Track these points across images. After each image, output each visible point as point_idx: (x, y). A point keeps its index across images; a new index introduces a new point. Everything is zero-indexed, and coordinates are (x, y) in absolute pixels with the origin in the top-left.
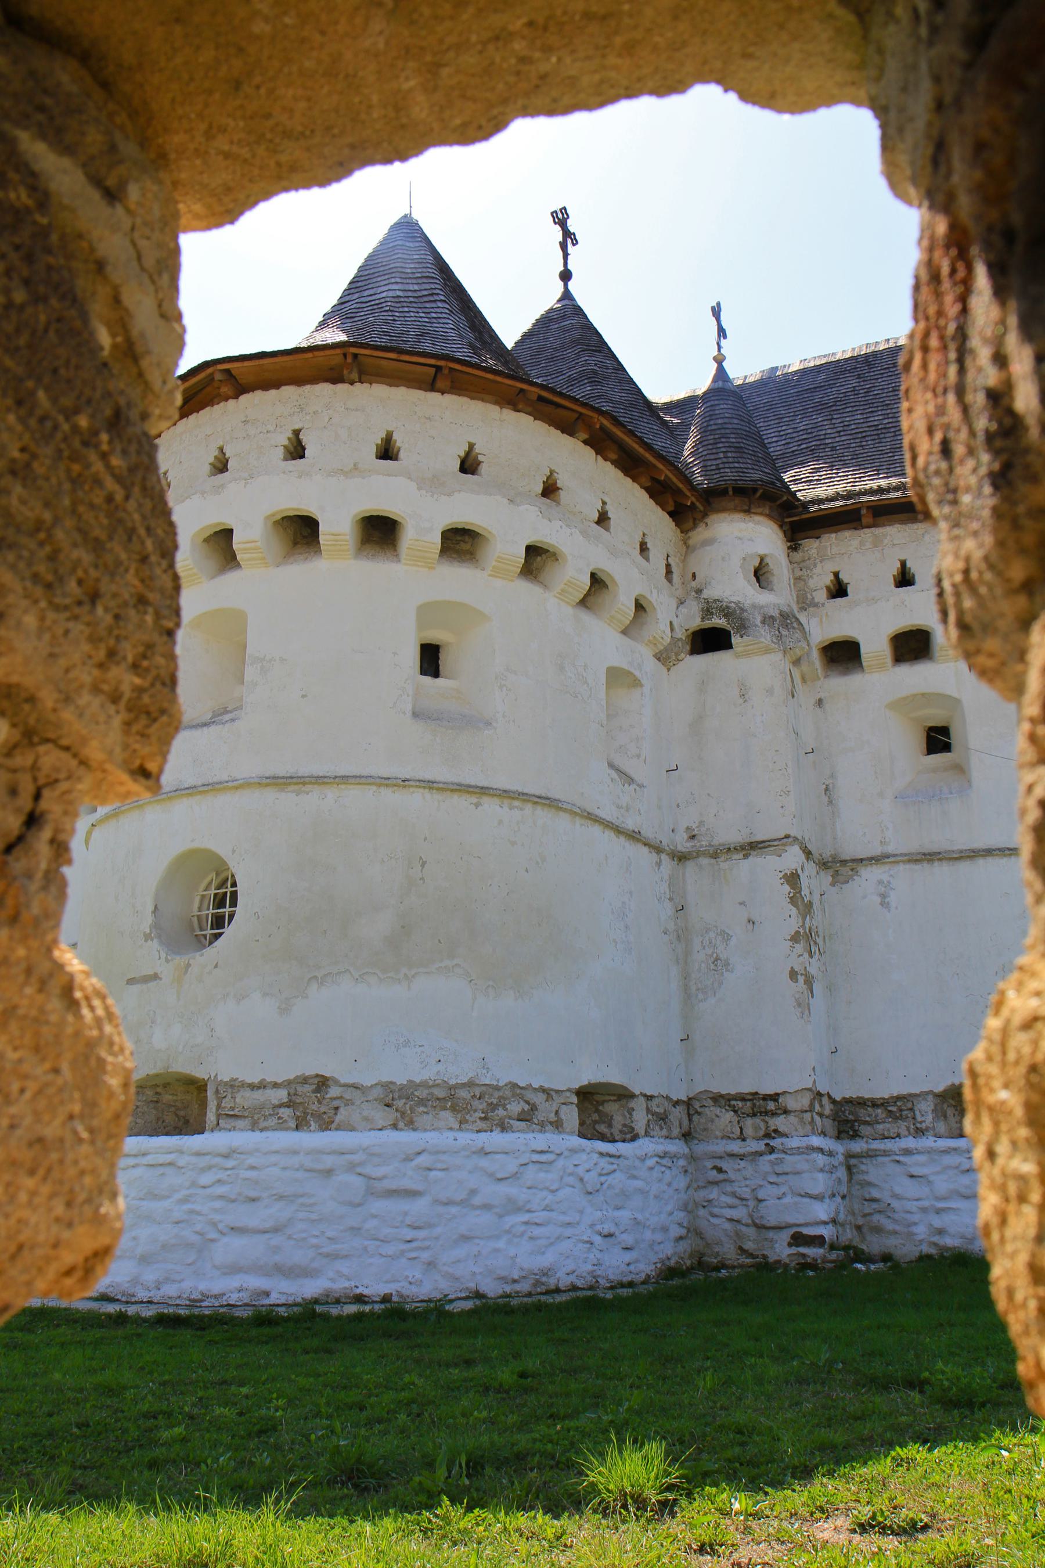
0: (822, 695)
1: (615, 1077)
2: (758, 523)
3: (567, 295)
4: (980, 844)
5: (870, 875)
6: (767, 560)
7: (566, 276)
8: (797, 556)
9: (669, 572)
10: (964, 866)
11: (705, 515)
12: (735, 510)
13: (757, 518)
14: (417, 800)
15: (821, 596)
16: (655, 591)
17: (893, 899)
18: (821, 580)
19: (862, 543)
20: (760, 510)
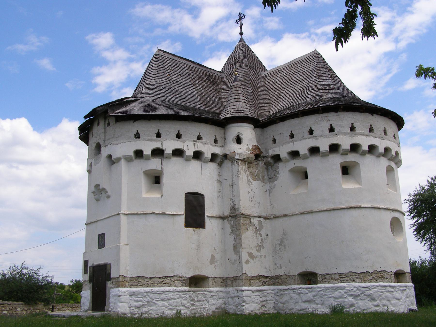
3: (241, 40)
7: (241, 34)
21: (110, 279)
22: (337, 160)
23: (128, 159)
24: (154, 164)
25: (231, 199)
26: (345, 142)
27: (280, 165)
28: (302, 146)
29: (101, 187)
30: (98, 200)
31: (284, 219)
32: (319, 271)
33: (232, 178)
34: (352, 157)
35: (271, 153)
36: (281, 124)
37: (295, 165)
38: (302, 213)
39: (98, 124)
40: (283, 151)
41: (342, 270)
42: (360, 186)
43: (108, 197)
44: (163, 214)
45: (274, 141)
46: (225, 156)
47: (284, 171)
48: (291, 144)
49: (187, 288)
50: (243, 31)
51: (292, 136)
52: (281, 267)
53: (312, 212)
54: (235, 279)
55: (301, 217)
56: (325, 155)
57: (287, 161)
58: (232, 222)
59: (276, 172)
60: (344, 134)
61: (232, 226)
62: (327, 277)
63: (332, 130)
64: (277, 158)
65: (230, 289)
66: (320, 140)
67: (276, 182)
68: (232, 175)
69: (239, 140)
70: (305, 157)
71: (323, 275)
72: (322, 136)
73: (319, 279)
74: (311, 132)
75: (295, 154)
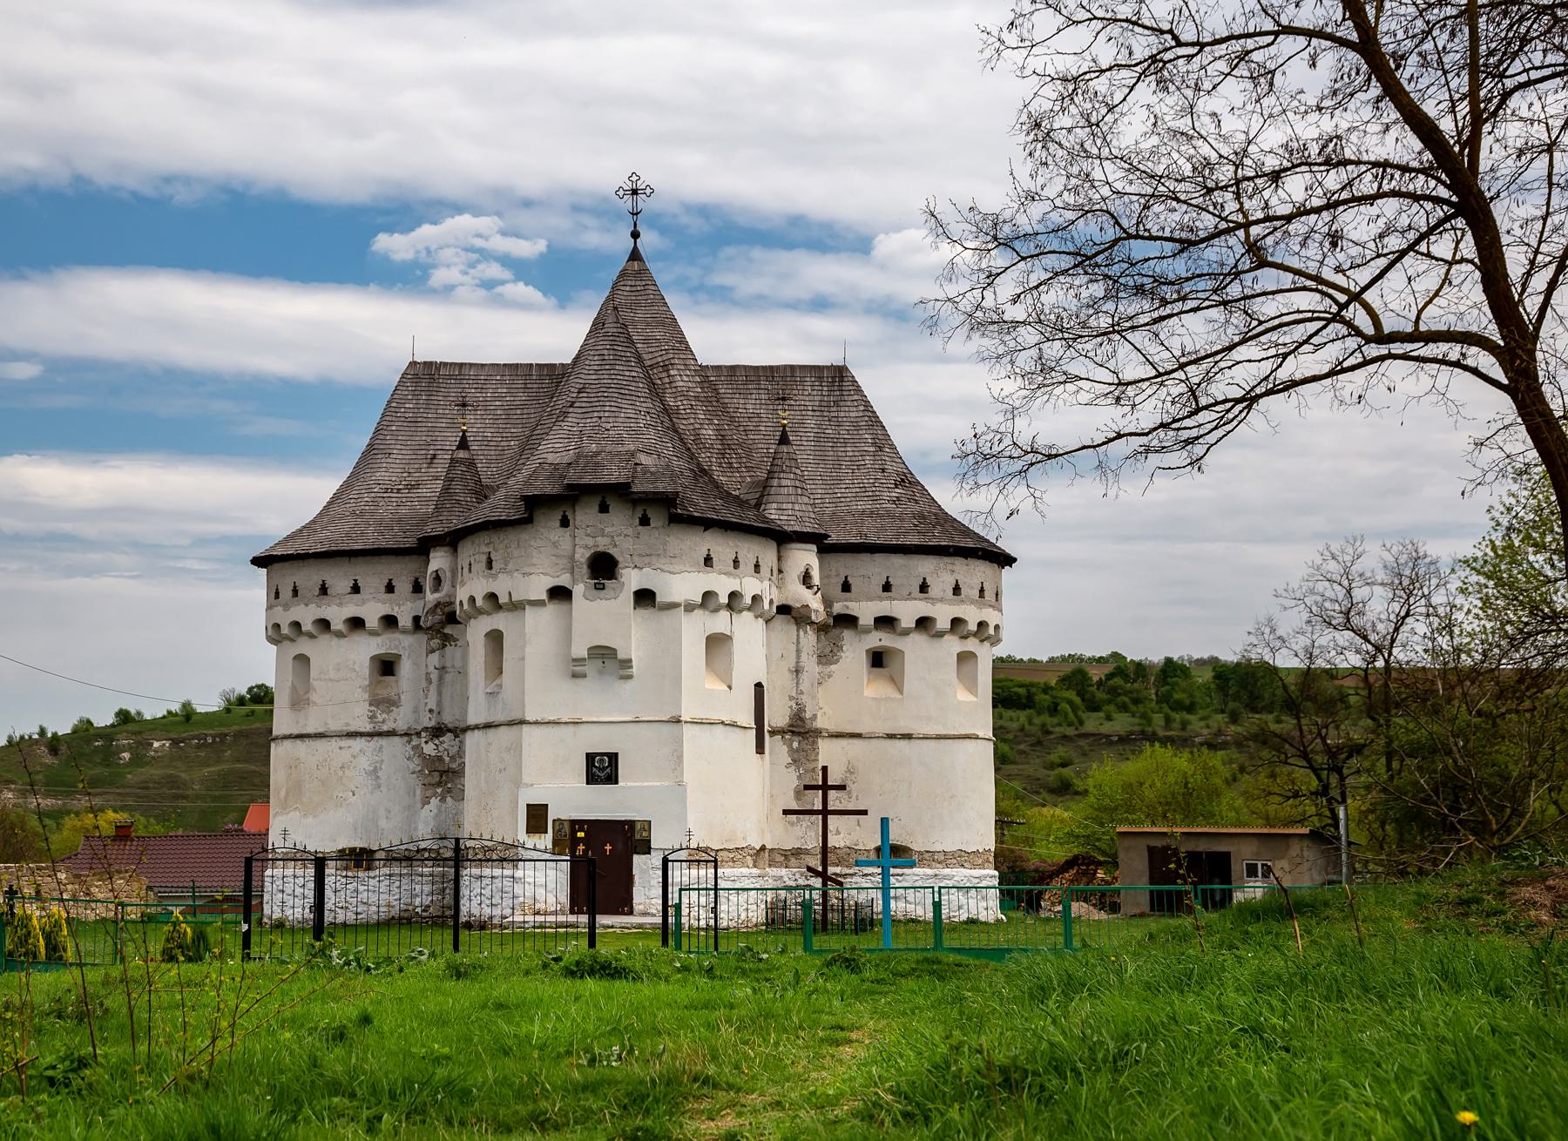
1: (359, 844)
3: (635, 255)
5: (469, 733)
9: (418, 588)
14: (287, 743)
21: (646, 848)
22: (953, 645)
23: (690, 608)
24: (720, 622)
25: (791, 698)
26: (972, 615)
27: (847, 634)
28: (907, 611)
29: (621, 655)
30: (575, 676)
31: (851, 741)
32: (917, 845)
33: (798, 657)
34: (972, 645)
35: (838, 608)
36: (865, 557)
37: (883, 643)
38: (891, 736)
39: (604, 509)
40: (867, 612)
41: (950, 847)
42: (972, 698)
43: (630, 677)
44: (734, 725)
45: (846, 587)
46: (784, 610)
47: (855, 650)
48: (886, 603)
49: (755, 871)
51: (887, 587)
52: (838, 833)
53: (908, 737)
54: (797, 853)
55: (889, 742)
56: (940, 635)
57: (867, 631)
58: (795, 745)
59: (837, 646)
60: (972, 602)
61: (791, 750)
62: (927, 856)
63: (957, 590)
64: (848, 621)
65: (783, 872)
66: (939, 605)
67: (833, 667)
68: (798, 651)
69: (806, 579)
70: (906, 632)
71: (920, 853)
72: (941, 600)
73: (915, 857)
74: (924, 588)
75: (886, 622)
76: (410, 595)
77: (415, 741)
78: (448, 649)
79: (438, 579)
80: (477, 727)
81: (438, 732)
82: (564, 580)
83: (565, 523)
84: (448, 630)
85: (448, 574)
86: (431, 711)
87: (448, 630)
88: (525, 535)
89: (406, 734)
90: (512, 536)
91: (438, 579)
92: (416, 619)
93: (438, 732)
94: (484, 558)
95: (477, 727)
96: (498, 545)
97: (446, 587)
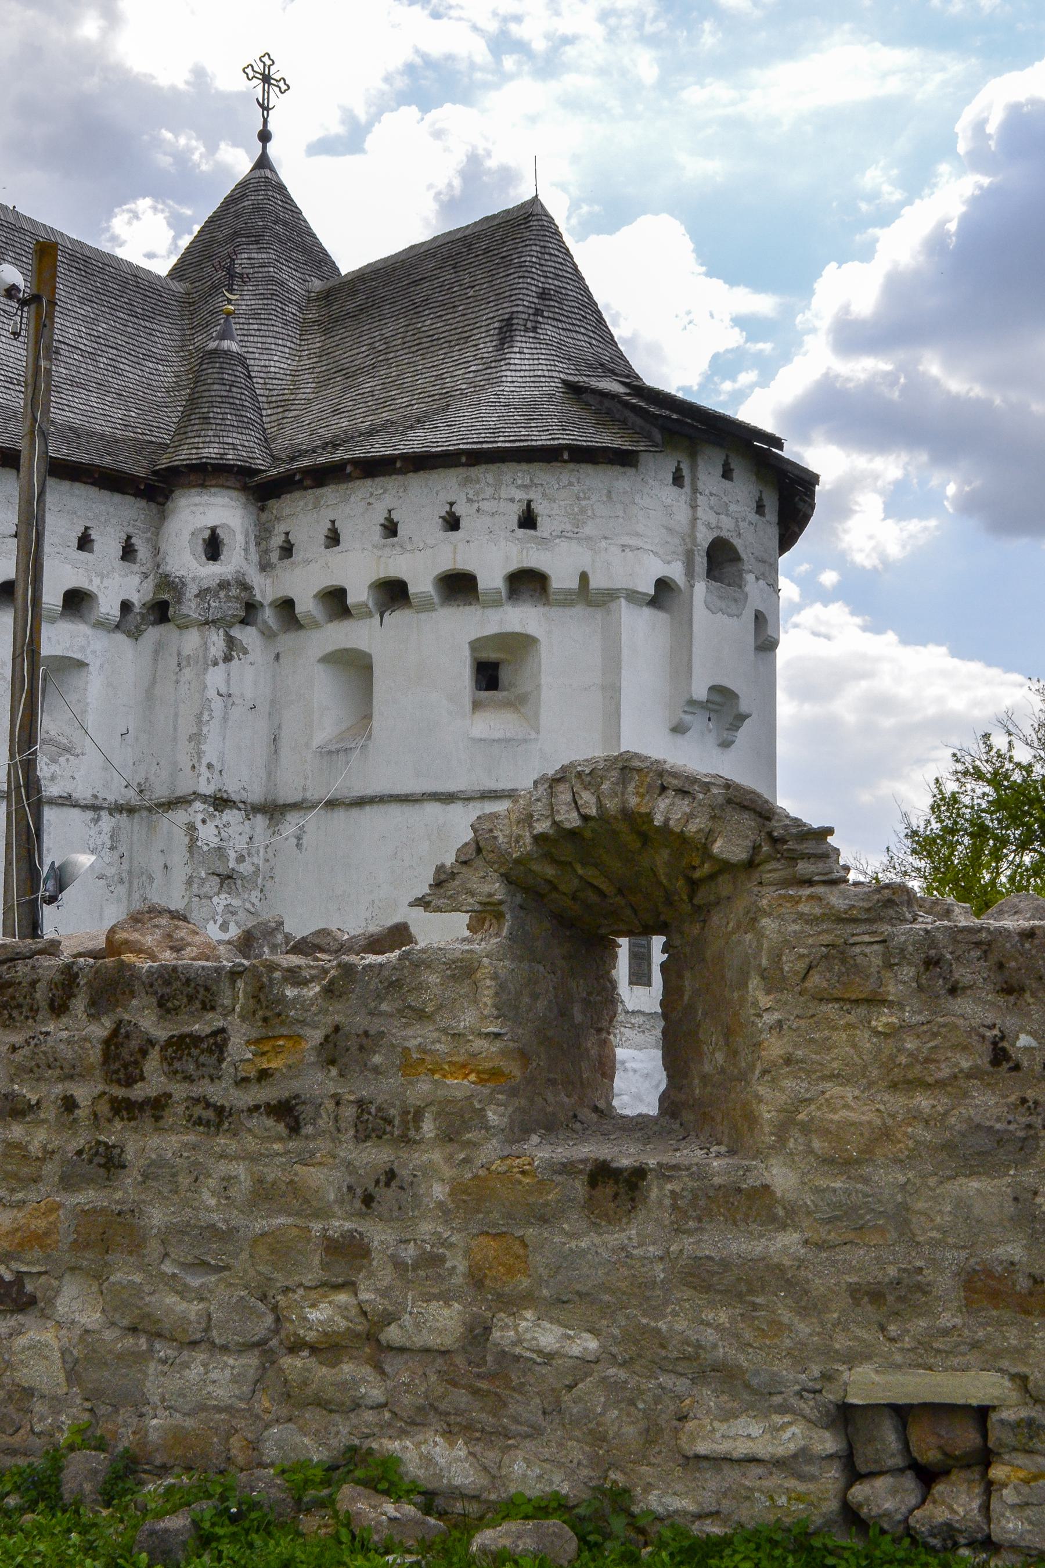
0: (280, 650)
2: (215, 494)
4: (369, 791)
6: (218, 531)
7: (265, 136)
8: (264, 516)
9: (128, 552)
10: (355, 812)
11: (172, 492)
12: (190, 486)
13: (213, 490)
15: (274, 556)
16: (96, 581)
17: (304, 841)
18: (277, 541)
19: (306, 505)
20: (214, 482)
50: (270, 127)
76: (118, 563)
77: (107, 822)
78: (235, 662)
79: (213, 547)
80: (296, 806)
81: (221, 802)
82: (676, 572)
83: (678, 480)
84: (237, 632)
85: (240, 538)
86: (210, 766)
87: (237, 632)
88: (620, 480)
89: (95, 808)
90: (594, 480)
91: (213, 547)
92: (126, 606)
93: (221, 802)
94: (514, 512)
95: (296, 806)
96: (556, 493)
97: (237, 559)
